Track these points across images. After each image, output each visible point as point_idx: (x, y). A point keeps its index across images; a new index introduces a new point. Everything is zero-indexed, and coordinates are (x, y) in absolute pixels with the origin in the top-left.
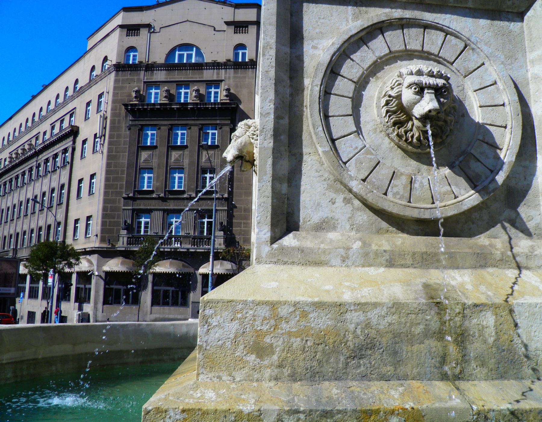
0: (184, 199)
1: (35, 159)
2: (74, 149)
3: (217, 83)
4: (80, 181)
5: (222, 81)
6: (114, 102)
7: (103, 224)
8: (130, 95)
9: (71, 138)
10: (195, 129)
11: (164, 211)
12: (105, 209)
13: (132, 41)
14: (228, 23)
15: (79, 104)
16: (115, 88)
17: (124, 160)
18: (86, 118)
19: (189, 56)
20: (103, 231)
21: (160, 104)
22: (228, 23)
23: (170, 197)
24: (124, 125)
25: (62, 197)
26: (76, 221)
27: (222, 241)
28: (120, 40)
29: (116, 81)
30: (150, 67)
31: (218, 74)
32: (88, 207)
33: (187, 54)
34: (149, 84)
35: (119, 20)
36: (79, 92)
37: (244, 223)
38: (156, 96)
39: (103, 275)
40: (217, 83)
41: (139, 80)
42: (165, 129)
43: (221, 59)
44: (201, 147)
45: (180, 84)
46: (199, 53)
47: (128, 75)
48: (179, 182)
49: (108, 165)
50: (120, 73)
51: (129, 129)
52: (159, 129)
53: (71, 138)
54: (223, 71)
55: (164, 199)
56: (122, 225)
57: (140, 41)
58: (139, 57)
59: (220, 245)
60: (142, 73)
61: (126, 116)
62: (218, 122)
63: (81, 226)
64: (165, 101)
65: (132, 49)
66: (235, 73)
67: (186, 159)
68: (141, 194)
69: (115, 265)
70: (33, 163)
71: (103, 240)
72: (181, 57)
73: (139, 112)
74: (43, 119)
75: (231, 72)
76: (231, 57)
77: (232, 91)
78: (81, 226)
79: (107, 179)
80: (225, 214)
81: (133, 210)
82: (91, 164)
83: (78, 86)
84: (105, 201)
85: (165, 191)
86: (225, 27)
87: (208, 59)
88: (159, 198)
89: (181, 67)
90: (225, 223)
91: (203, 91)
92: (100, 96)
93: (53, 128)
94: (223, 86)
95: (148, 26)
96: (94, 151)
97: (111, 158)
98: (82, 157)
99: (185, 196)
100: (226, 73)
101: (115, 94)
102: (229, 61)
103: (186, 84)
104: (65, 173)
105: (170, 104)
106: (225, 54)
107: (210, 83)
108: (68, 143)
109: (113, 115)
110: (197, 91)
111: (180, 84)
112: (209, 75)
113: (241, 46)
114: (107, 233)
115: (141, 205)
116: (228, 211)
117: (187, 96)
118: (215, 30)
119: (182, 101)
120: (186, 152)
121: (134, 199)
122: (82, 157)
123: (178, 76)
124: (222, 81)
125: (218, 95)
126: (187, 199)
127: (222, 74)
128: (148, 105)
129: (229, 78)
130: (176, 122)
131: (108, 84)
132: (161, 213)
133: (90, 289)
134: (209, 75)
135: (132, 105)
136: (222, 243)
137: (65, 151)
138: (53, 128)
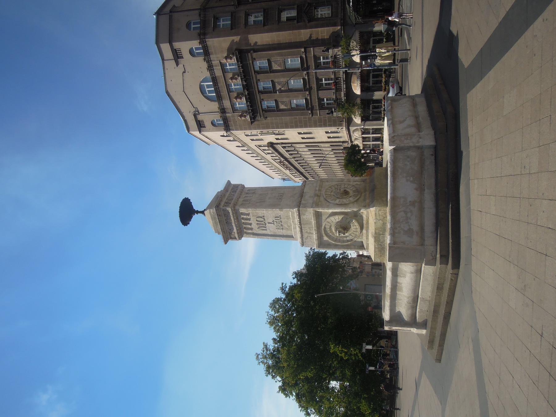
0: (309, 79)
1: (290, 160)
2: (282, 143)
3: (223, 66)
4: (303, 138)
5: (220, 63)
6: (250, 129)
7: (330, 126)
8: (244, 120)
9: (275, 146)
10: (259, 76)
11: (318, 90)
12: (320, 126)
13: (208, 124)
14: (177, 64)
15: (253, 145)
16: (241, 130)
17: (287, 119)
18: (262, 140)
19: (208, 86)
20: (335, 125)
21: (247, 102)
22: (177, 64)
23: (308, 87)
24: (265, 121)
25: (314, 146)
26: (329, 138)
27: (336, 50)
28: (209, 131)
29: (237, 130)
30: (223, 111)
31: (216, 66)
32: (320, 134)
33: (207, 88)
34: (234, 110)
35: (197, 133)
36: (244, 145)
37: (321, 33)
38: (241, 104)
39: (363, 122)
40: (223, 66)
41: (233, 116)
42: (263, 96)
43: (205, 65)
44: (271, 70)
45: (229, 91)
46: (205, 80)
47: (231, 123)
48: (296, 83)
49: (292, 127)
50: (230, 128)
51: (266, 118)
52: (263, 100)
53: (275, 146)
54: (213, 62)
55: (310, 90)
56: (331, 115)
57: (206, 119)
58: (217, 117)
59: (339, 51)
60: (227, 115)
61: (258, 121)
62: (251, 62)
63: (332, 135)
64: (244, 99)
65: (213, 124)
66: (212, 54)
67: (280, 80)
68: (309, 107)
69: (357, 120)
70: (293, 161)
71: (341, 125)
72: (210, 92)
73: (255, 114)
74: (263, 158)
75: (212, 57)
76: (201, 58)
77: (225, 55)
78: (332, 135)
79: (301, 127)
80: (317, 49)
81: (320, 110)
82: (292, 135)
83: (241, 145)
84: (316, 126)
85: (305, 91)
86: (181, 66)
87: (207, 74)
88: (310, 94)
89: (217, 91)
90: (323, 48)
91: (230, 75)
92: (247, 135)
93: (268, 153)
94: (224, 61)
95: (195, 115)
96: (283, 134)
97: (287, 127)
98: (286, 139)
99: (306, 78)
100: (214, 61)
101: (246, 129)
102: (205, 59)
103: (228, 86)
104: (298, 146)
105: (245, 96)
106: (200, 64)
107: (224, 71)
108: (279, 147)
109: (258, 128)
110: (232, 79)
111: (229, 91)
112: (218, 72)
113: (191, 52)
114: (336, 123)
115: (316, 104)
116: (314, 47)
117: (237, 85)
118: (184, 72)
119: (241, 87)
120: (276, 80)
121: (312, 109)
122: (286, 139)
123: (224, 92)
124: (220, 63)
125: (232, 64)
126: (308, 76)
127: (215, 62)
128: (249, 110)
129: (218, 57)
130: (257, 90)
131: (240, 134)
132: (320, 92)
133: (373, 129)
134: (218, 72)
135: (251, 119)
136: (337, 49)
137: (284, 147)
138: (268, 153)
